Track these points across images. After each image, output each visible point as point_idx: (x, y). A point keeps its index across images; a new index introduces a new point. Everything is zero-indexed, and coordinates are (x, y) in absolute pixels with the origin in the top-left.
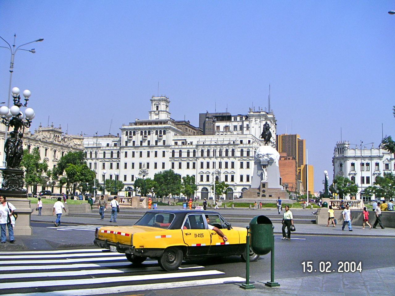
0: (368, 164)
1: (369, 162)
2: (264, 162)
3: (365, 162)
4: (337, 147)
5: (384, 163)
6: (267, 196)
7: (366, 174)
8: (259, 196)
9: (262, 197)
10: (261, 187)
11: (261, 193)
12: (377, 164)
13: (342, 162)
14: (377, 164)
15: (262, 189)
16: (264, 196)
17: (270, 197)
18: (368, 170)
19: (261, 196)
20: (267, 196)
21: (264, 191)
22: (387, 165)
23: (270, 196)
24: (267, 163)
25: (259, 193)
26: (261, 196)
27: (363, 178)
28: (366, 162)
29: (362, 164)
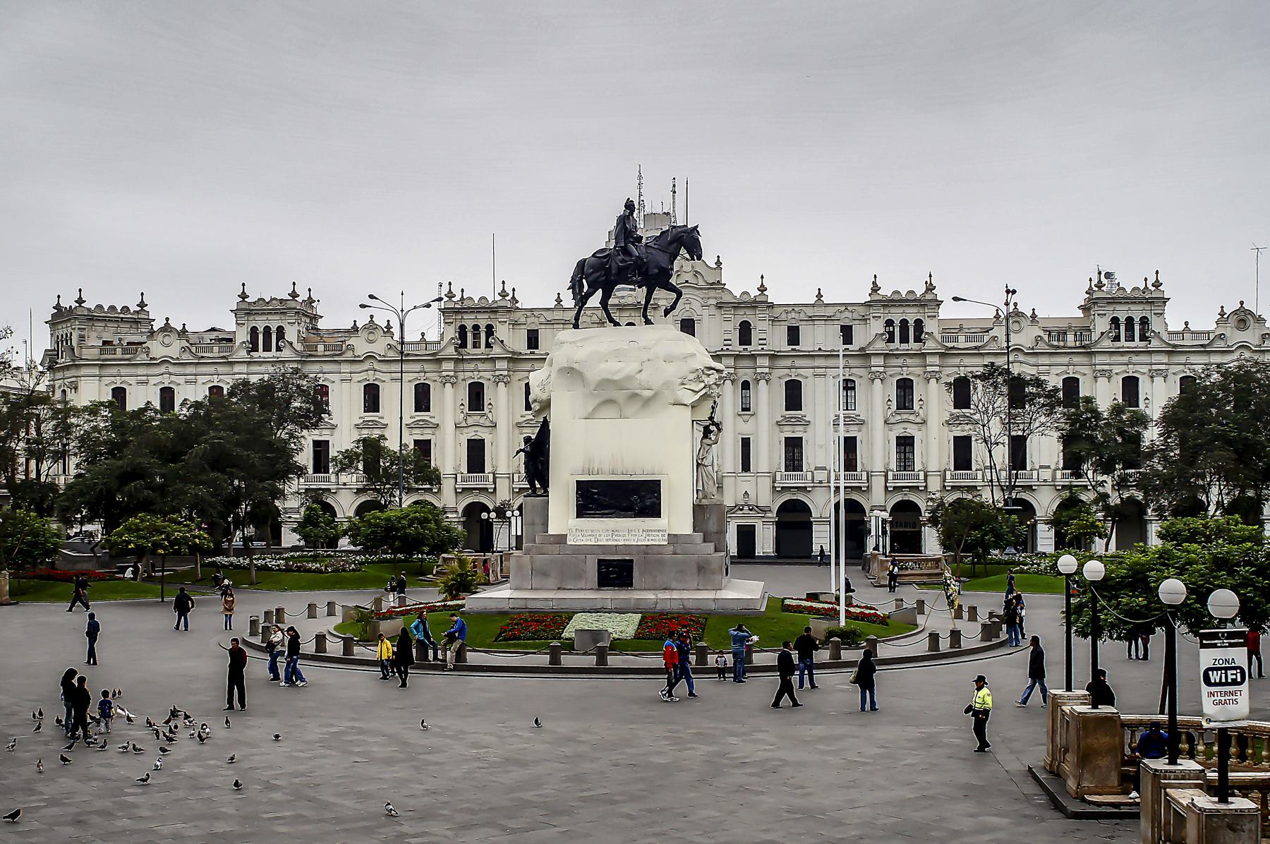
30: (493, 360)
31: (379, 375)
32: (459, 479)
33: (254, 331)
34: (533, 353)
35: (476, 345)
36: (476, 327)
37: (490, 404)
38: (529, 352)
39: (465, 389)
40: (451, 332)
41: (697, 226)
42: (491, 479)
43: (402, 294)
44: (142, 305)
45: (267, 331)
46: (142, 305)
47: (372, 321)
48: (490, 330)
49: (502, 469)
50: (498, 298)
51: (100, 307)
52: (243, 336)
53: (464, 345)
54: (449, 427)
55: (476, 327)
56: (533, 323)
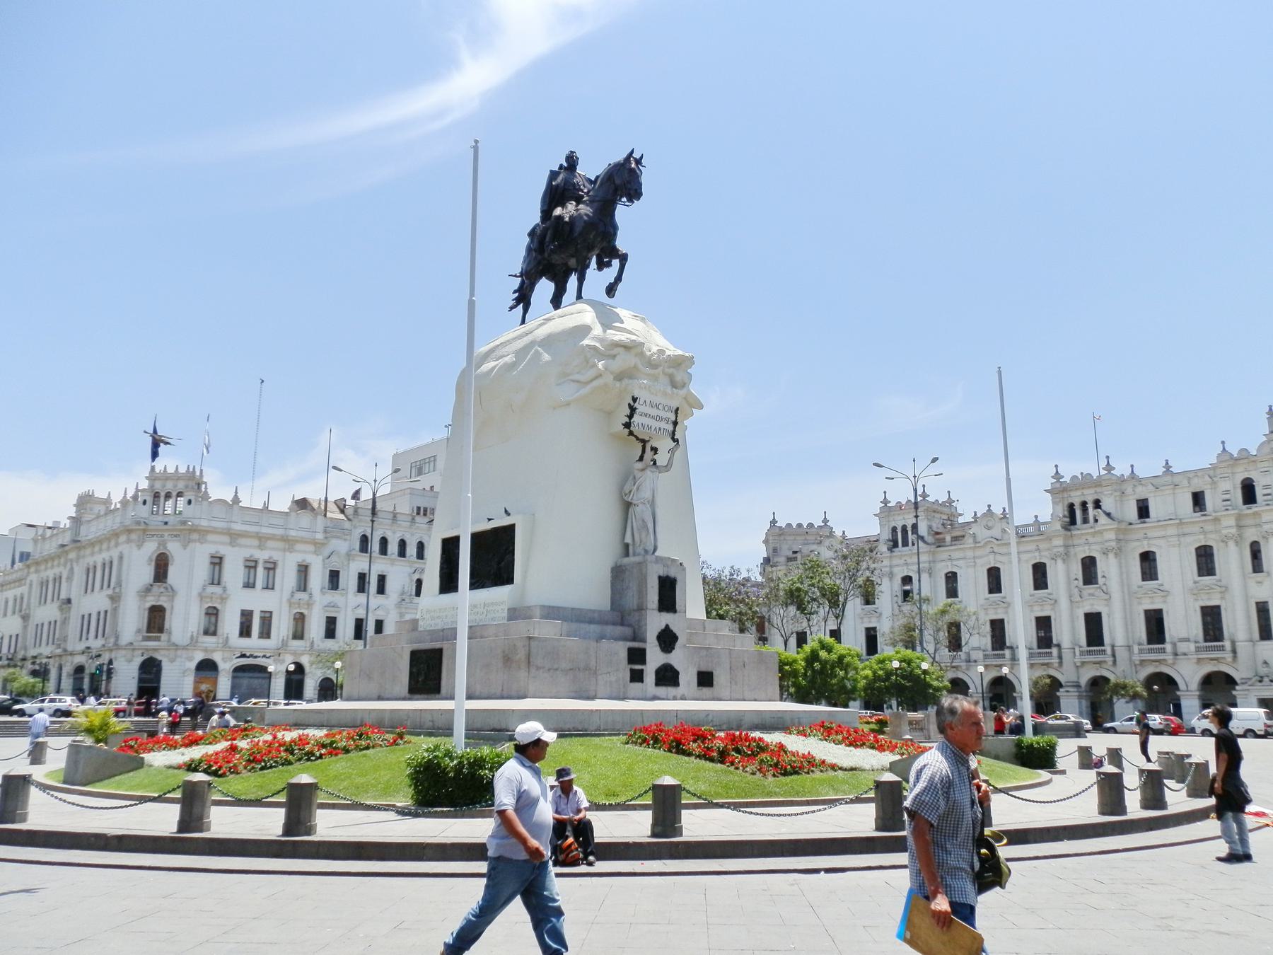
0: (271, 567)
1: (276, 556)
2: (654, 412)
3: (261, 555)
4: (151, 486)
5: (324, 567)
6: (688, 678)
7: (258, 601)
8: (637, 677)
9: (657, 684)
10: (653, 597)
11: (655, 657)
12: (304, 570)
13: (173, 548)
14: (304, 570)
15: (655, 621)
16: (667, 677)
17: (706, 691)
18: (269, 587)
19: (650, 677)
20: (688, 678)
21: (667, 640)
22: (334, 577)
23: (705, 679)
24: (670, 428)
25: (637, 656)
26: (650, 677)
27: (246, 616)
28: (266, 557)
29: (251, 565)
30: (1100, 532)
31: (999, 558)
32: (1077, 653)
33: (894, 530)
34: (1145, 522)
35: (1085, 521)
36: (1084, 504)
37: (1104, 577)
38: (1139, 521)
39: (1077, 563)
40: (1062, 511)
41: (632, 152)
42: (1109, 651)
43: (914, 461)
44: (825, 521)
45: (904, 529)
46: (825, 521)
47: (989, 510)
48: (1097, 504)
49: (1120, 640)
50: (1103, 472)
51: (789, 525)
52: (887, 535)
53: (1073, 521)
54: (1064, 603)
55: (1084, 504)
56: (1142, 493)
